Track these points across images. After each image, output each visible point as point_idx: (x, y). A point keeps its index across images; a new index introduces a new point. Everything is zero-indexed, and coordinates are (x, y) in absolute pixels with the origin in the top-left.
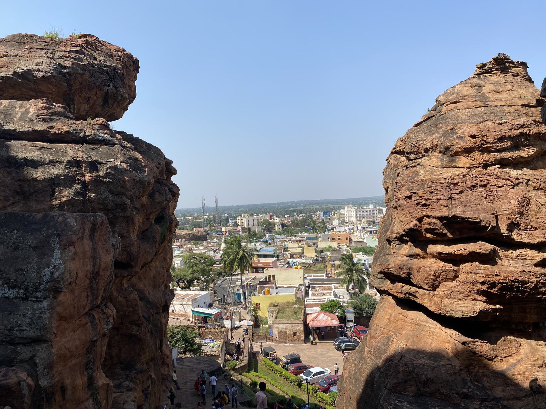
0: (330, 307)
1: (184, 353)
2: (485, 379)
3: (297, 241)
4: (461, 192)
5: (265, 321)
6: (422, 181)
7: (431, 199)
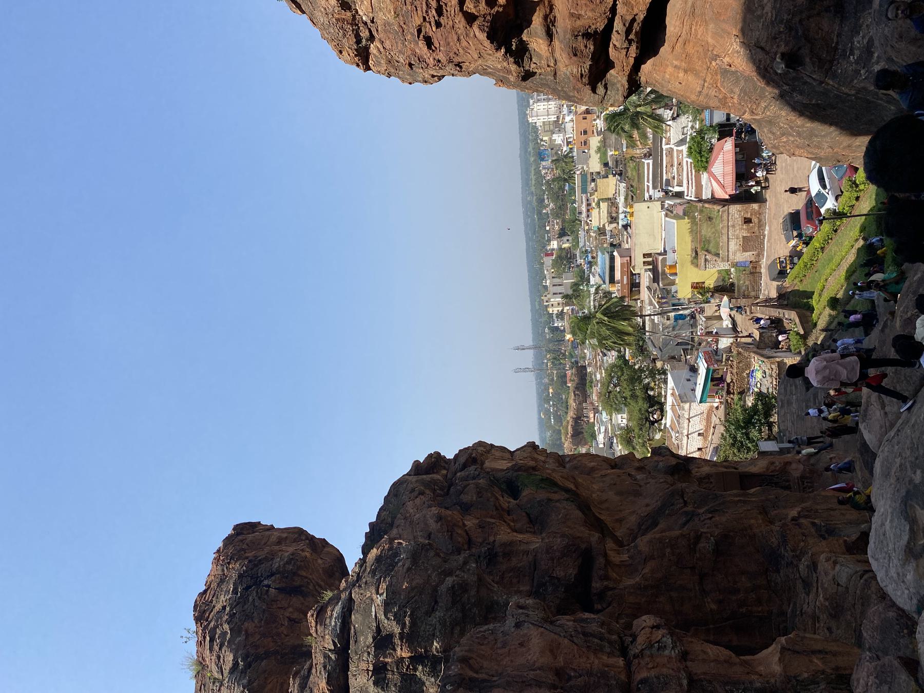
0: (702, 155)
1: (770, 425)
3: (588, 211)
5: (724, 274)
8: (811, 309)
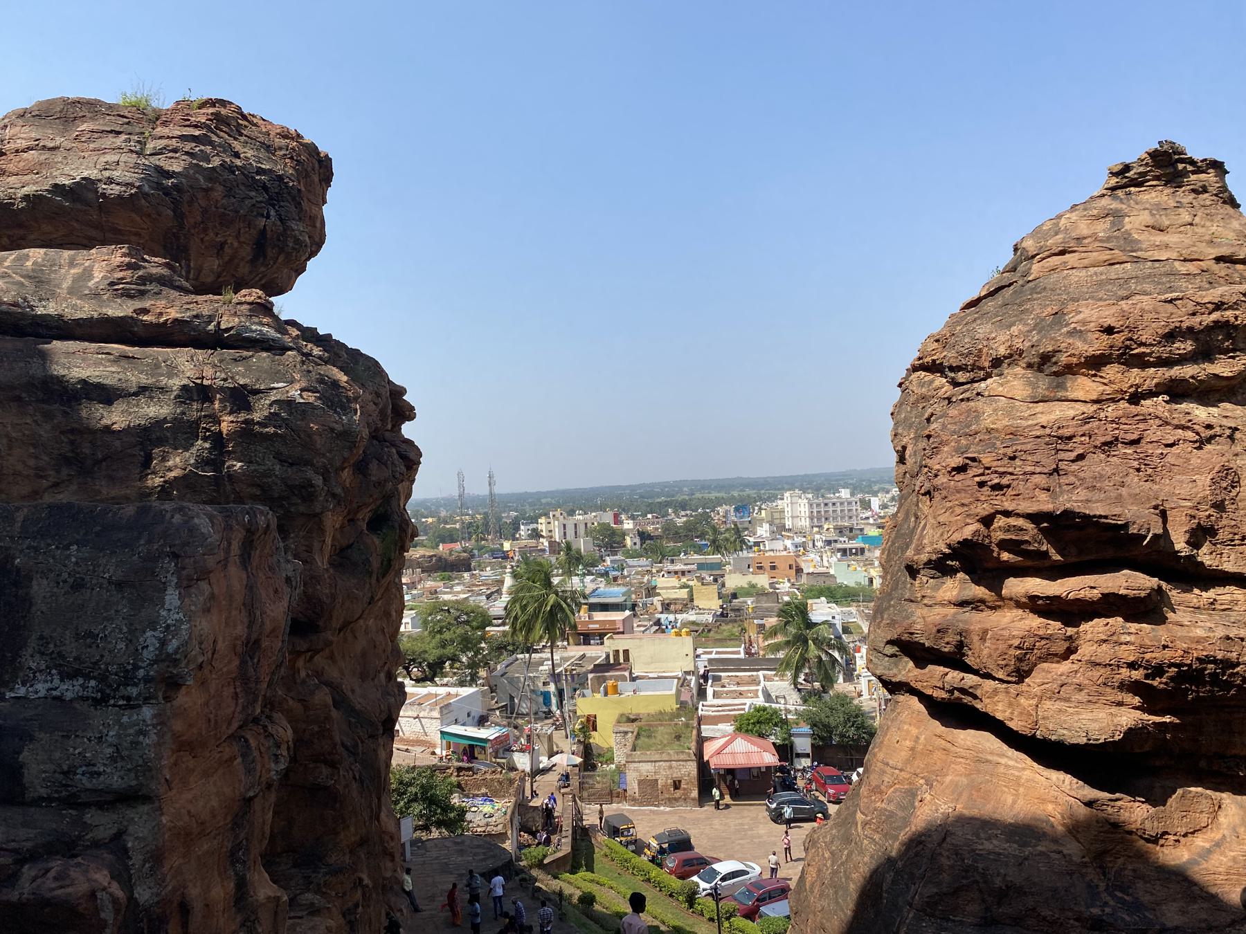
0: (756, 724)
1: (426, 828)
2: (1140, 885)
3: (676, 573)
4: (1081, 457)
5: (608, 755)
6: (989, 431)
7: (1011, 474)
8: (574, 871)
